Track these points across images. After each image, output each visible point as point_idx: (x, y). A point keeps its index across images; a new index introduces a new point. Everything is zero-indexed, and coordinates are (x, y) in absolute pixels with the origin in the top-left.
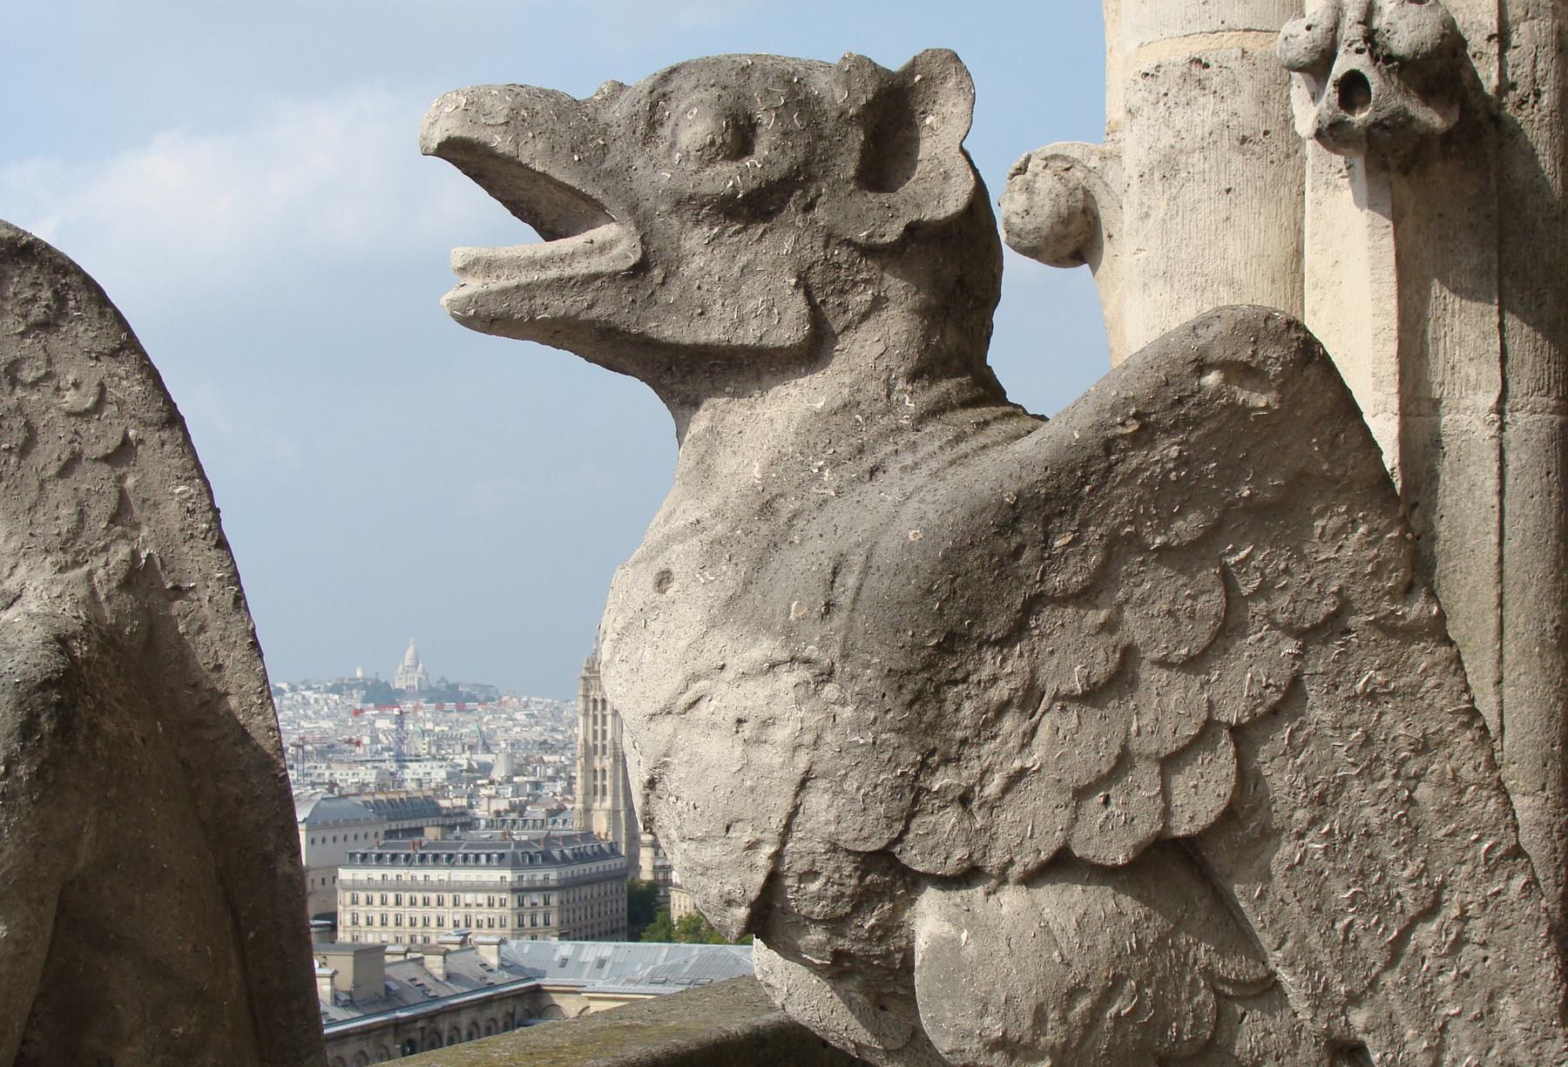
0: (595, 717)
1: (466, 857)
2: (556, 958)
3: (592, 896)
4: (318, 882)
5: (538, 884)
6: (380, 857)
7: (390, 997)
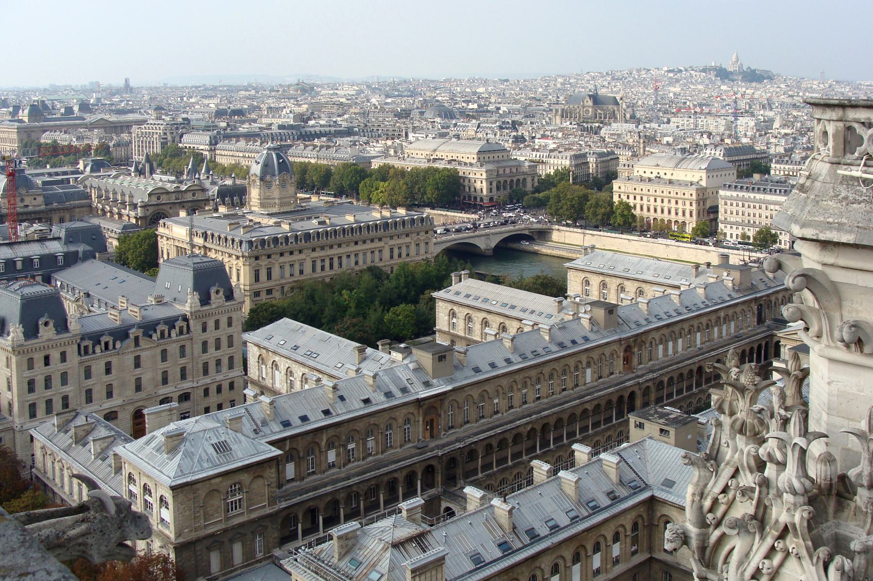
1: (771, 190)
4: (711, 193)
6: (736, 187)
7: (753, 288)
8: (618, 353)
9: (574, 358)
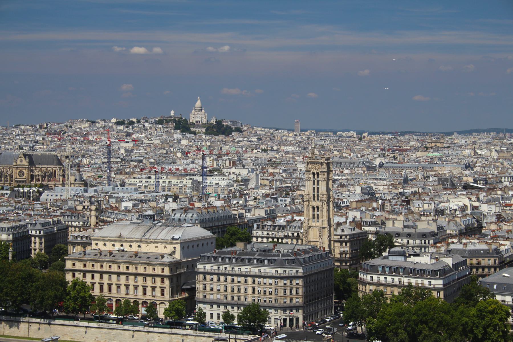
0: (314, 181)
3: (318, 279)
5: (293, 275)
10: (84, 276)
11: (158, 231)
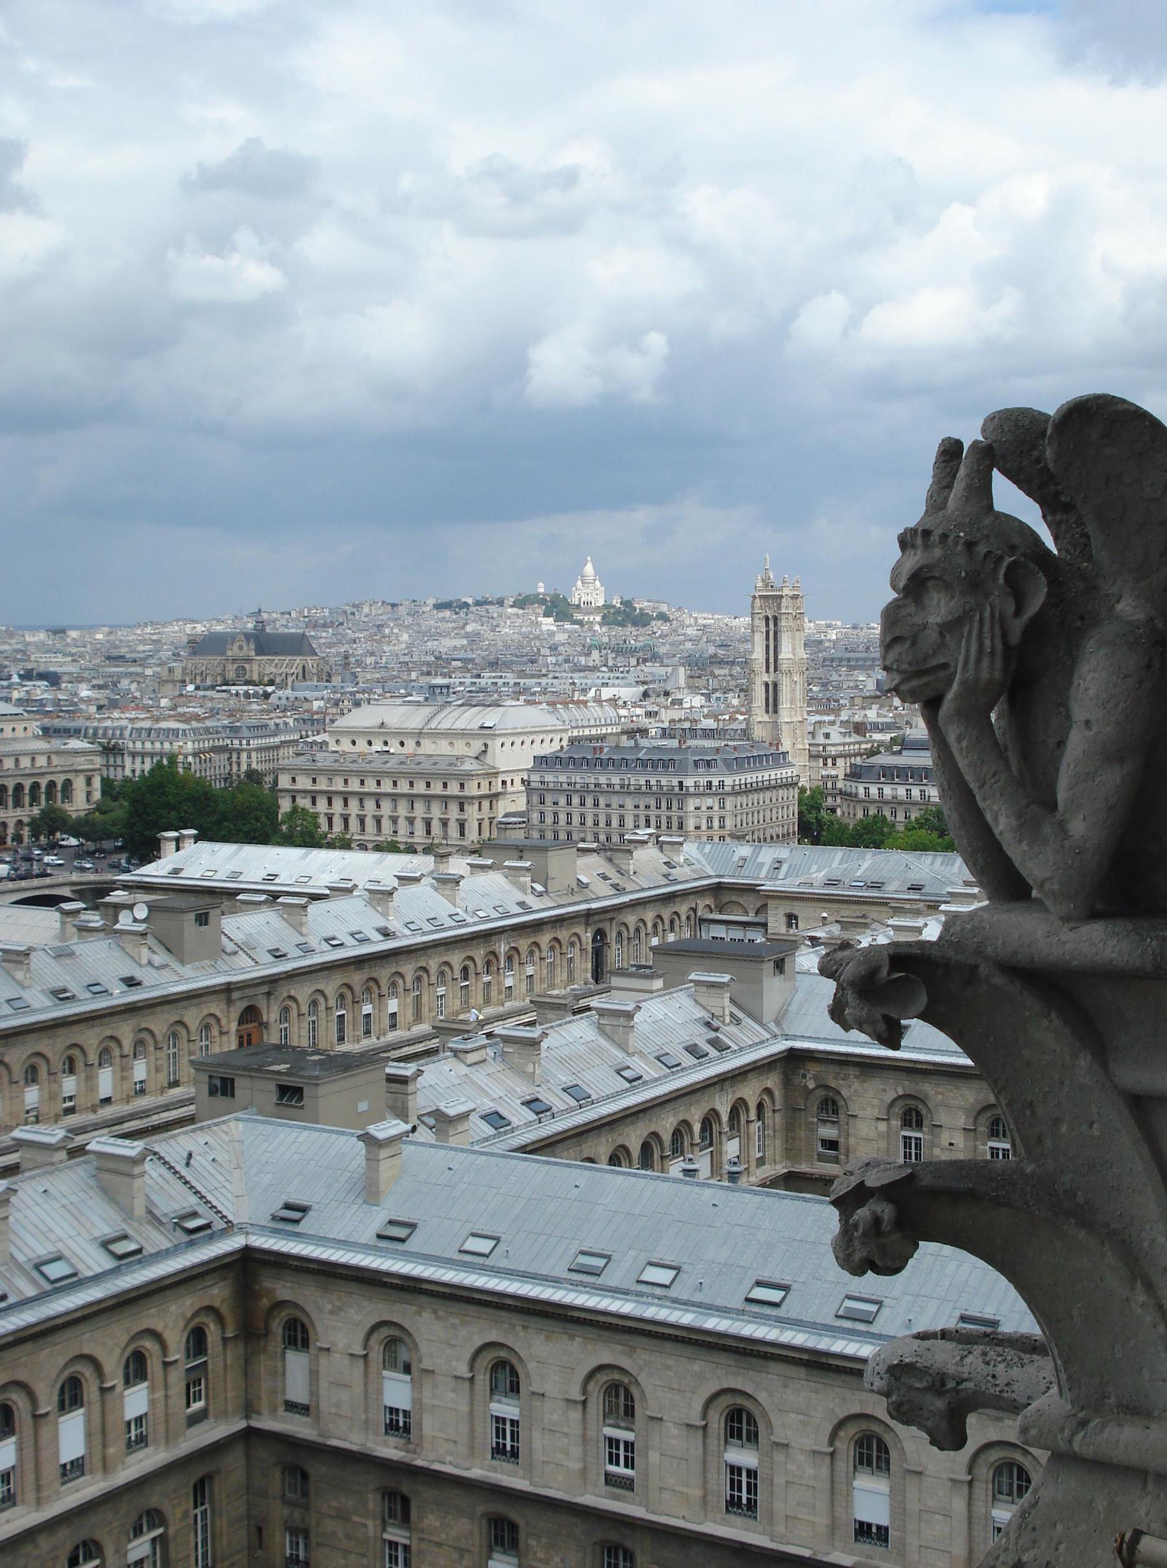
2: (735, 858)
8: (224, 1022)
9: (97, 1030)
10: (314, 803)
11: (455, 714)
